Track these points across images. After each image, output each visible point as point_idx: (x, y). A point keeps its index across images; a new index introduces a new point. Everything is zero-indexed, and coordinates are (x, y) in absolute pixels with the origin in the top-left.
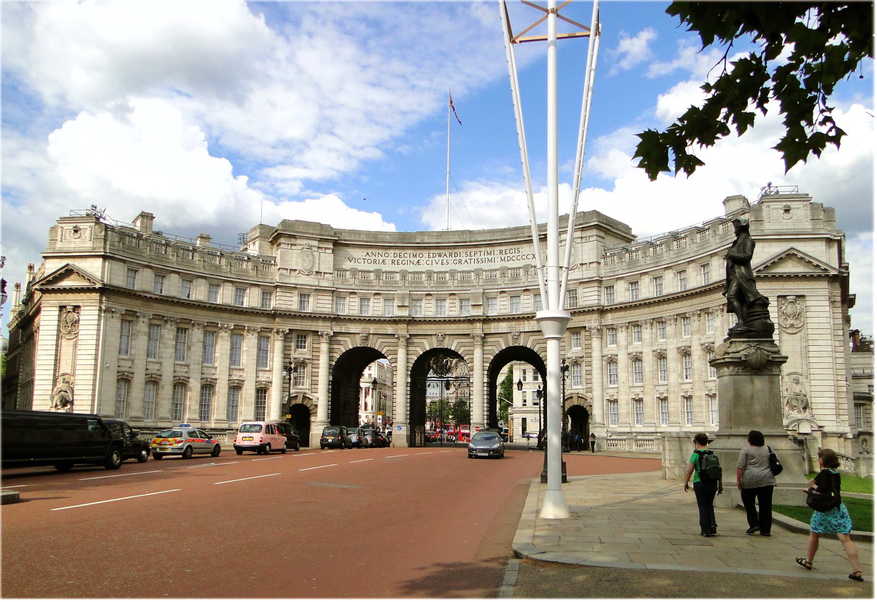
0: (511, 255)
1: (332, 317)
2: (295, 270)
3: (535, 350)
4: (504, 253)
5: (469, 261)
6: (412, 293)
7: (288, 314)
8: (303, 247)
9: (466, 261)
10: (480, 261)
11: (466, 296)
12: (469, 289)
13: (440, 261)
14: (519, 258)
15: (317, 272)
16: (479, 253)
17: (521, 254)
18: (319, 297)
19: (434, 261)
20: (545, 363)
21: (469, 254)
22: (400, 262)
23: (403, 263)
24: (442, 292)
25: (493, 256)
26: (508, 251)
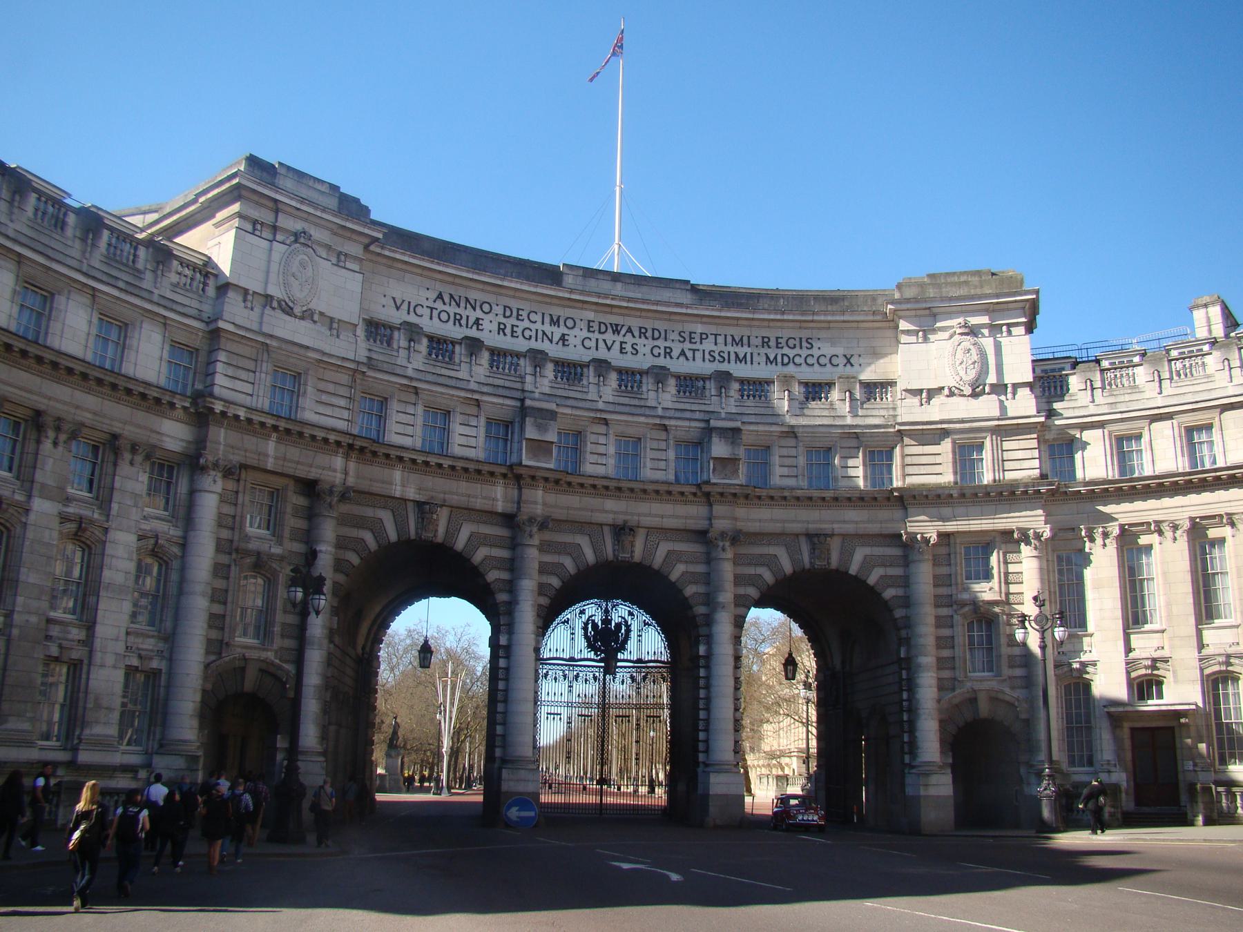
0: (791, 353)
1: (358, 443)
2: (268, 298)
3: (872, 580)
4: (772, 343)
5: (689, 354)
6: (561, 410)
7: (242, 413)
8: (292, 238)
9: (683, 353)
10: (717, 357)
11: (694, 435)
12: (697, 415)
13: (617, 346)
14: (810, 361)
15: (321, 314)
16: (712, 338)
17: (816, 352)
18: (322, 385)
19: (601, 344)
20: (899, 613)
21: (686, 335)
22: (519, 330)
23: (527, 333)
24: (636, 419)
25: (746, 349)
26: (783, 341)
